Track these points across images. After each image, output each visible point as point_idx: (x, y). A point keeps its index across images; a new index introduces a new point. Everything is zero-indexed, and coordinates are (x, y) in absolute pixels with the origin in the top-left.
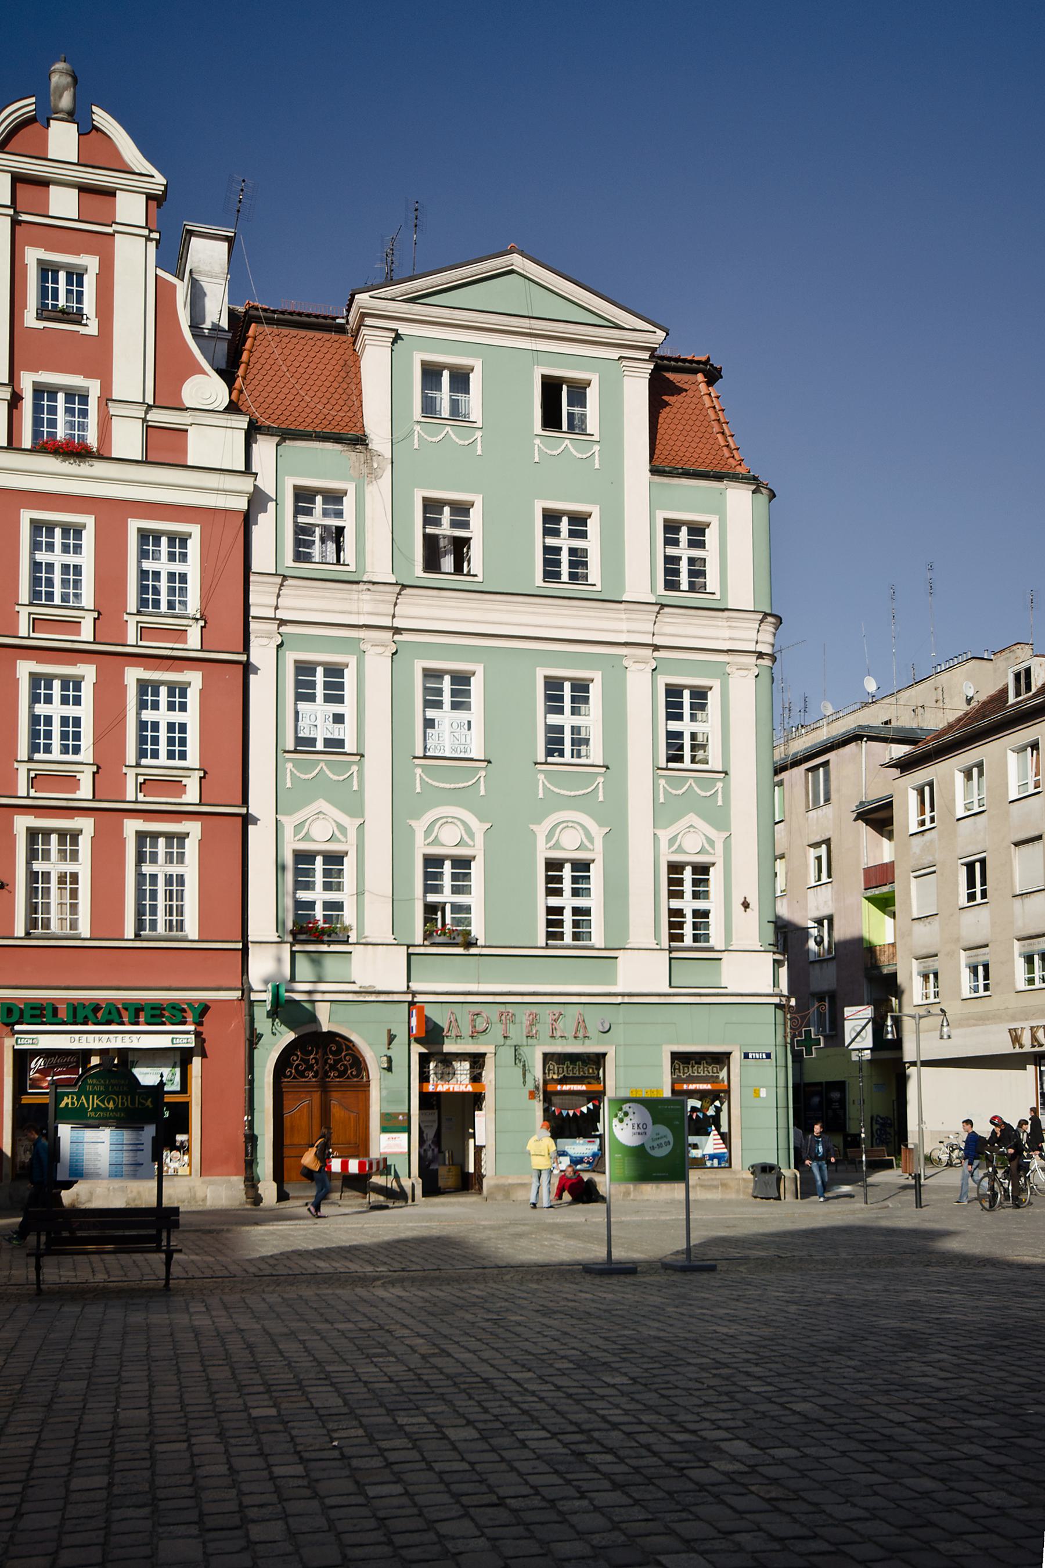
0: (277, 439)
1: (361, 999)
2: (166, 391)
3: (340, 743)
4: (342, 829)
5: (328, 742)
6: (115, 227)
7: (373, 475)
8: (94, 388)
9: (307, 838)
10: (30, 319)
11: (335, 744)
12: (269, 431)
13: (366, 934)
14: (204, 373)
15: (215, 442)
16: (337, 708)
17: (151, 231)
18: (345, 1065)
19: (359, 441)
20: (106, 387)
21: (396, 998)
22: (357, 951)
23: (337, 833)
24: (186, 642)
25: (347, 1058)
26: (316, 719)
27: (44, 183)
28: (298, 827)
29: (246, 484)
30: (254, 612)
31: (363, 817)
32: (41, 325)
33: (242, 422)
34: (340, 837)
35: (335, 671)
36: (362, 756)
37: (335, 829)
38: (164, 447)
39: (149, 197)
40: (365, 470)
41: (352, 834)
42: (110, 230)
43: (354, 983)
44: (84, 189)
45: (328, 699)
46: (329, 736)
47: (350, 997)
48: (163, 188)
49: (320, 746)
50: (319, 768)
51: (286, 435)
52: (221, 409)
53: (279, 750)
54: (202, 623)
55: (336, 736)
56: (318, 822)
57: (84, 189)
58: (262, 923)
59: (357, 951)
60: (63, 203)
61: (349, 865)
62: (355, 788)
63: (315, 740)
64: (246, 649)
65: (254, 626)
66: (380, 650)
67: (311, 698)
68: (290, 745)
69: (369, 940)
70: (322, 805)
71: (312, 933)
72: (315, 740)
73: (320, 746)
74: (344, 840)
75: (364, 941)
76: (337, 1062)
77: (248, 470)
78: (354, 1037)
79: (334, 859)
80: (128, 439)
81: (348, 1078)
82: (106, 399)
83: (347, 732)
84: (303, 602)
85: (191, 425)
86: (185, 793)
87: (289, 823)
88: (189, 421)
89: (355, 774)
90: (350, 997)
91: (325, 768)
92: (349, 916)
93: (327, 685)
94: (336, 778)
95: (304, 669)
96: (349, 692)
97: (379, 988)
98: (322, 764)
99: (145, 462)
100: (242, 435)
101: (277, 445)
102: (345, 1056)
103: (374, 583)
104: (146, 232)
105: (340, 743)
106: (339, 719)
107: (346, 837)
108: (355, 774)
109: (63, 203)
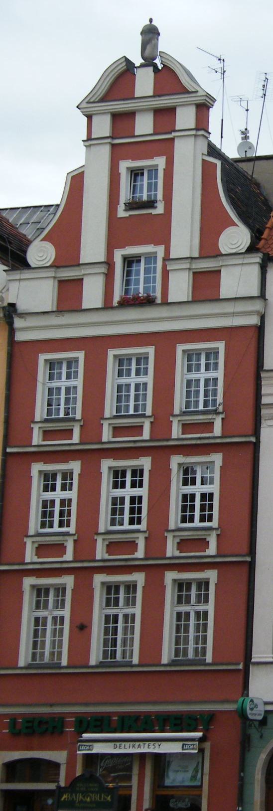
6: (174, 134)
8: (160, 250)
10: (122, 213)
14: (235, 224)
30: (265, 400)
32: (127, 214)
33: (257, 258)
38: (206, 286)
44: (158, 112)
60: (144, 125)
65: (264, 412)
82: (167, 259)
109: (144, 125)
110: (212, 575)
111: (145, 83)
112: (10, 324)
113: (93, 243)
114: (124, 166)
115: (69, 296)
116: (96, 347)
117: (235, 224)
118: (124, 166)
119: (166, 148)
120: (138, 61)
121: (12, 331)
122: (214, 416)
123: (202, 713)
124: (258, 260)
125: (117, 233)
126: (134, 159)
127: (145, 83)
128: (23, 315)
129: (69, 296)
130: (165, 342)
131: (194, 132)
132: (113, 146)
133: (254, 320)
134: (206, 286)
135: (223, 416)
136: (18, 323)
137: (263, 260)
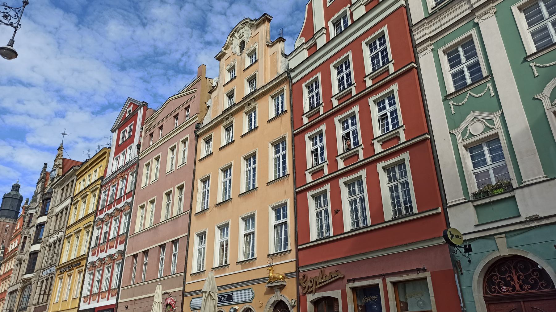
18: (533, 279)
28: (464, 133)
31: (501, 108)
35: (468, 44)
41: (498, 122)
47: (522, 227)
50: (468, 95)
53: (446, 98)
59: (518, 194)
62: (493, 94)
74: (493, 127)
78: (530, 256)
81: (540, 289)
90: (522, 227)
91: (471, 93)
97: (541, 215)
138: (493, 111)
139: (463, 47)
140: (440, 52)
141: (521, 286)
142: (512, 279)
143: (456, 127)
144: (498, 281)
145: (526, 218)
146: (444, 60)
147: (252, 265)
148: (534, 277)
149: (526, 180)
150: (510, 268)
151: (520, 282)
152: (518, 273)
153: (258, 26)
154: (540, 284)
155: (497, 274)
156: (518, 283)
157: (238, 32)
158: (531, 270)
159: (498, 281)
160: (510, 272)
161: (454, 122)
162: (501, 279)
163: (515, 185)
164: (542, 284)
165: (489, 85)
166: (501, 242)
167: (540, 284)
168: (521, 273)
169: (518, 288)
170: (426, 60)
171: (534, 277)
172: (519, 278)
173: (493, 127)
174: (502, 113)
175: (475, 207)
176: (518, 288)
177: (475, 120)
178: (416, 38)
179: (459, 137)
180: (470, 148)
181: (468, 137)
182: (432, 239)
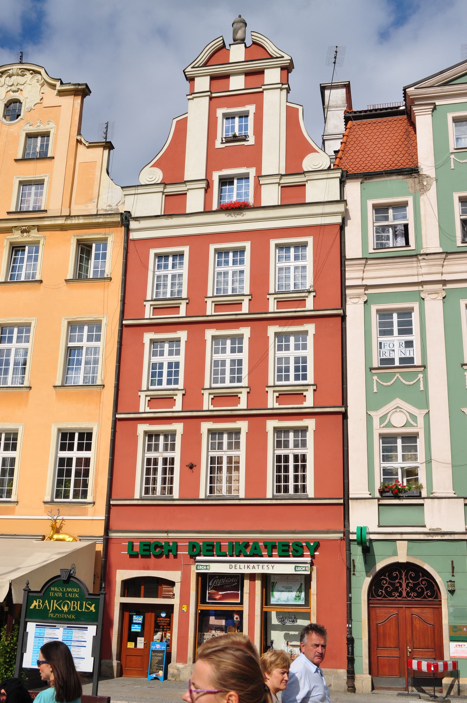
0: (360, 180)
1: (430, 538)
2: (294, 166)
3: (411, 360)
4: (414, 417)
5: (402, 360)
6: (263, 87)
7: (424, 189)
8: (252, 172)
9: (390, 425)
10: (218, 144)
11: (407, 361)
12: (354, 176)
13: (433, 491)
14: (315, 151)
15: (322, 189)
16: (408, 338)
17: (283, 84)
18: (421, 588)
19: (413, 171)
20: (259, 170)
21: (456, 537)
22: (427, 503)
23: (410, 420)
24: (305, 307)
25: (424, 582)
26: (394, 346)
27: (226, 76)
28: (382, 419)
29: (340, 208)
30: (348, 283)
34: (412, 423)
35: (406, 314)
36: (425, 367)
37: (409, 417)
38: (293, 195)
39: (283, 68)
40: (418, 187)
41: (421, 421)
42: (261, 90)
43: (424, 526)
44: (248, 74)
45: (401, 332)
46: (403, 356)
48: (289, 61)
49: (397, 363)
50: (396, 378)
51: (366, 176)
52: (326, 168)
54: (314, 294)
55: (408, 355)
56: (396, 414)
57: (248, 74)
58: (358, 485)
59: (427, 503)
60: (237, 83)
61: (420, 443)
62: (422, 388)
63: (393, 359)
64: (343, 305)
65: (348, 292)
66: (434, 296)
67: (390, 333)
68: (376, 364)
69: (436, 495)
70: (398, 402)
71: (398, 491)
72: (393, 359)
73: (397, 363)
74: (415, 424)
75: (432, 496)
76: (415, 585)
77: (342, 200)
78: (427, 567)
79: (410, 439)
80: (271, 195)
81: (425, 598)
82: (259, 176)
83: (415, 353)
84: (380, 274)
85: (307, 181)
86: (305, 401)
87: (376, 416)
88: (305, 179)
89: (421, 379)
91: (400, 377)
92: (422, 478)
93: (400, 324)
94: (408, 383)
95: (384, 314)
96: (416, 327)
97: (444, 530)
98: (398, 375)
99: (282, 206)
100: (338, 180)
101: (361, 183)
102: (422, 581)
103: (427, 254)
104: (280, 86)
105: (411, 360)
106: (409, 344)
107: (416, 423)
108: (421, 379)
109: (237, 83)
110: (310, 423)
111: (237, 53)
112: (127, 227)
113: (195, 165)
114: (220, 112)
115: (174, 206)
116: (199, 242)
117: (315, 151)
118: (220, 112)
119: (257, 97)
120: (229, 40)
121: (128, 231)
122: (307, 294)
123: (308, 542)
124: (339, 175)
125: (213, 159)
126: (228, 107)
127: (237, 53)
128: (137, 219)
129: (174, 206)
130: (260, 237)
131: (280, 86)
132: (211, 98)
133: (338, 219)
134: (293, 195)
135: (314, 294)
136: (133, 225)
137: (342, 176)
138: (419, 407)
139: (399, 316)
140: (374, 308)
141: (408, 593)
142: (401, 585)
143: (376, 409)
144: (386, 585)
145: (430, 529)
146: (375, 319)
147: (12, 512)
148: (422, 586)
149: (438, 492)
150: (401, 574)
151: (408, 589)
152: (408, 580)
153: (61, 93)
154: (425, 593)
155: (387, 579)
156: (402, 589)
157: (10, 76)
158: (420, 579)
159: (386, 585)
160: (401, 578)
161: (373, 401)
162: (390, 583)
163: (424, 494)
164: (427, 593)
165: (421, 376)
166: (402, 547)
167: (425, 593)
168: (411, 581)
169: (404, 594)
170: (354, 310)
171: (422, 586)
172: (407, 585)
173: (415, 424)
174: (428, 413)
175: (379, 505)
176: (404, 594)
177: (398, 410)
178: (348, 275)
179: (376, 422)
180: (385, 438)
181: (386, 426)
182: (327, 532)
